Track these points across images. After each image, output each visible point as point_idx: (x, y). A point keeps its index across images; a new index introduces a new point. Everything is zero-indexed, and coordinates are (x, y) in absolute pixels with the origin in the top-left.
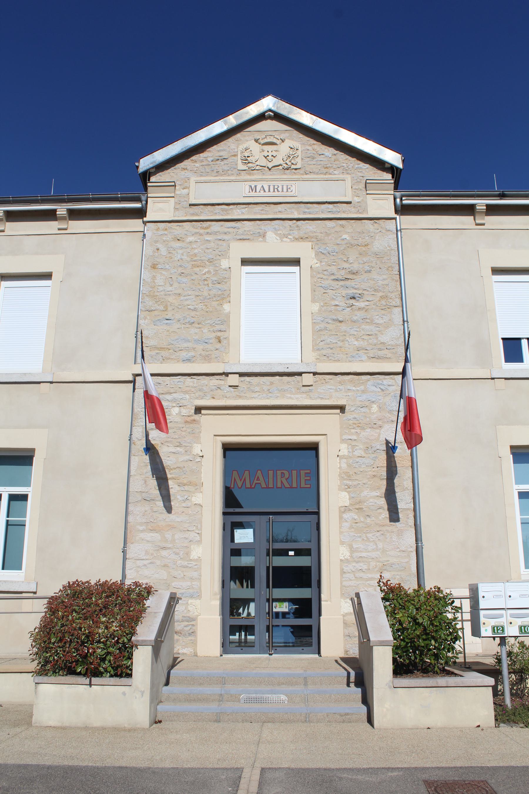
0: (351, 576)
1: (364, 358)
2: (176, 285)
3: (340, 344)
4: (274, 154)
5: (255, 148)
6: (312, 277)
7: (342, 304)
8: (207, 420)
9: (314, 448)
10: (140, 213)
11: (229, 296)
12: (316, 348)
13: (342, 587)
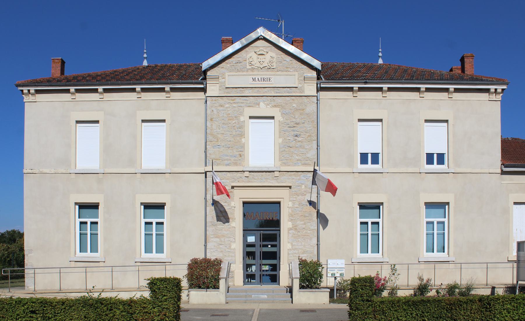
0: (292, 255)
1: (300, 164)
2: (221, 129)
3: (290, 158)
4: (263, 60)
5: (255, 56)
6: (279, 125)
7: (292, 139)
8: (236, 191)
9: (279, 203)
10: (204, 90)
11: (244, 135)
12: (280, 160)
13: (288, 259)
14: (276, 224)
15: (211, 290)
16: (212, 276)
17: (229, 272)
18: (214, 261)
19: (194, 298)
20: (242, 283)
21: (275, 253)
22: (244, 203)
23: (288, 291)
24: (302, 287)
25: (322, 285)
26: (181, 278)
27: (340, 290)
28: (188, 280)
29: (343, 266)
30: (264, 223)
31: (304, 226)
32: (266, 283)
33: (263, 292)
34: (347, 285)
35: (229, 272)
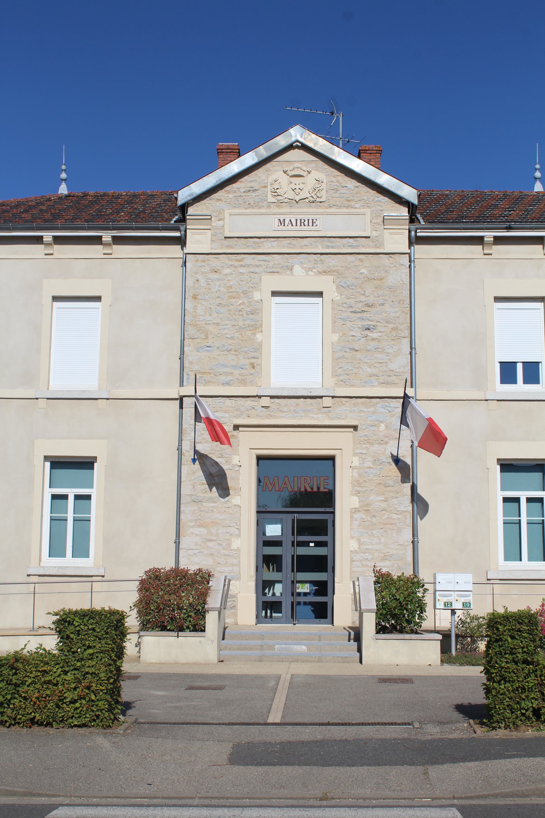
8: (243, 436)
9: (332, 459)
13: (351, 572)
14: (327, 499)
15: (187, 633)
16: (190, 604)
17: (225, 596)
18: (196, 574)
19: (152, 651)
20: (253, 620)
21: (325, 558)
22: (260, 458)
23: (352, 636)
24: (381, 630)
25: (426, 624)
26: (126, 610)
27: (464, 637)
28: (139, 612)
29: (470, 587)
30: (302, 505)
31: (384, 505)
32: (305, 620)
33: (298, 639)
34: (480, 626)
35: (225, 596)
